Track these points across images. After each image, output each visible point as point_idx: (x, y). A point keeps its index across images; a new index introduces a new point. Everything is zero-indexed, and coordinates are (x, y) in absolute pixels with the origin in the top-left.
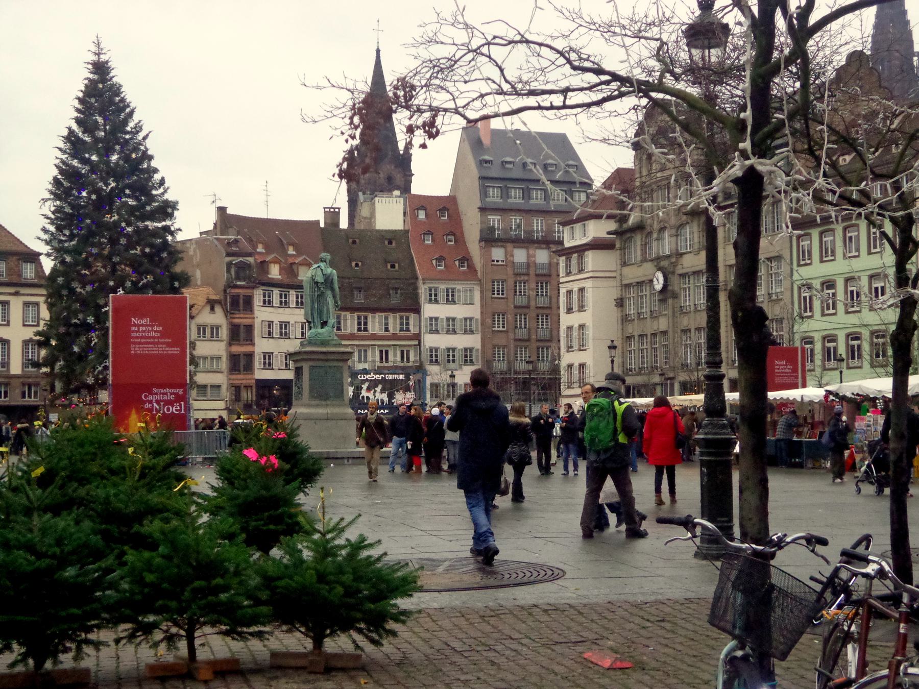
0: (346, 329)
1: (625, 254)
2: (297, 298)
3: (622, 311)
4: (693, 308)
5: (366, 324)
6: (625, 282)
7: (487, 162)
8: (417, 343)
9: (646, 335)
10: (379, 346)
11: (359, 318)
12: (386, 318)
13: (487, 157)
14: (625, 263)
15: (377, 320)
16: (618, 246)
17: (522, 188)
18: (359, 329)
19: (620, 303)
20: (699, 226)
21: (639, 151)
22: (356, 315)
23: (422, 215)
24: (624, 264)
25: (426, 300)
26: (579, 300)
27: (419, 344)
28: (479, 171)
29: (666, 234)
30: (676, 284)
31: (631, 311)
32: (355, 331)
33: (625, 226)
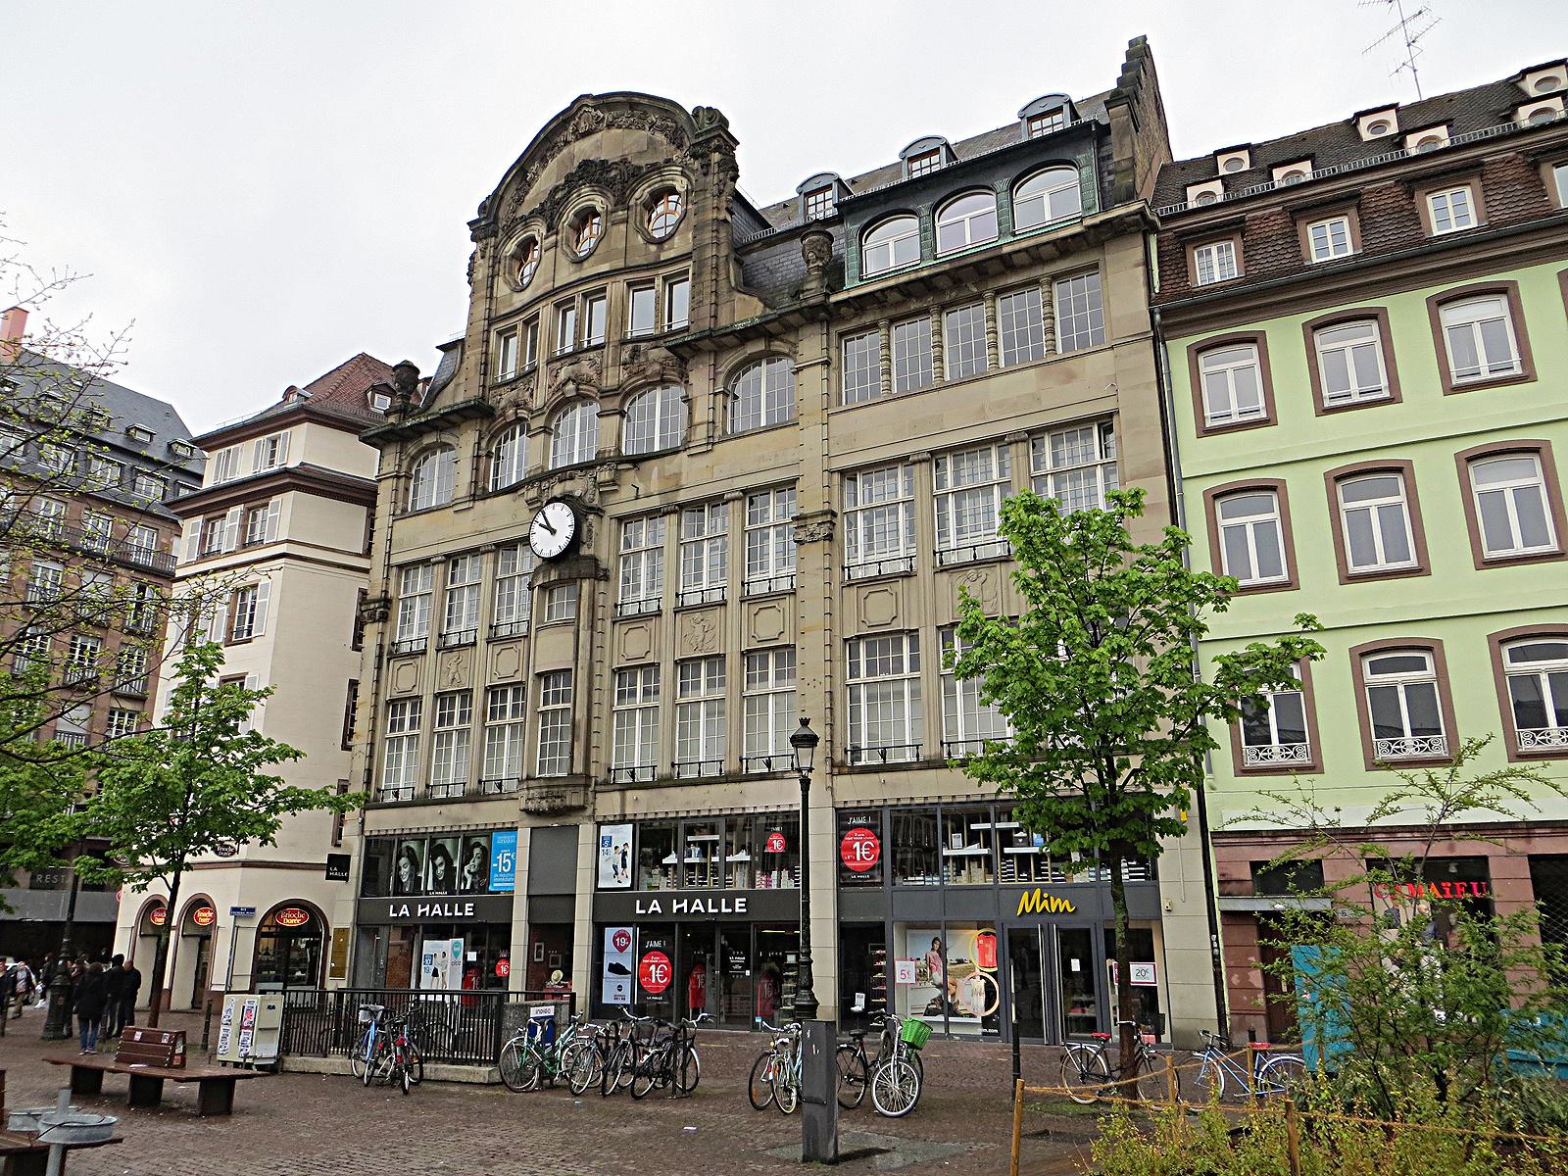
1: (407, 489)
6: (396, 560)
9: (466, 694)
19: (375, 610)
26: (231, 617)
30: (603, 545)
31: (415, 628)
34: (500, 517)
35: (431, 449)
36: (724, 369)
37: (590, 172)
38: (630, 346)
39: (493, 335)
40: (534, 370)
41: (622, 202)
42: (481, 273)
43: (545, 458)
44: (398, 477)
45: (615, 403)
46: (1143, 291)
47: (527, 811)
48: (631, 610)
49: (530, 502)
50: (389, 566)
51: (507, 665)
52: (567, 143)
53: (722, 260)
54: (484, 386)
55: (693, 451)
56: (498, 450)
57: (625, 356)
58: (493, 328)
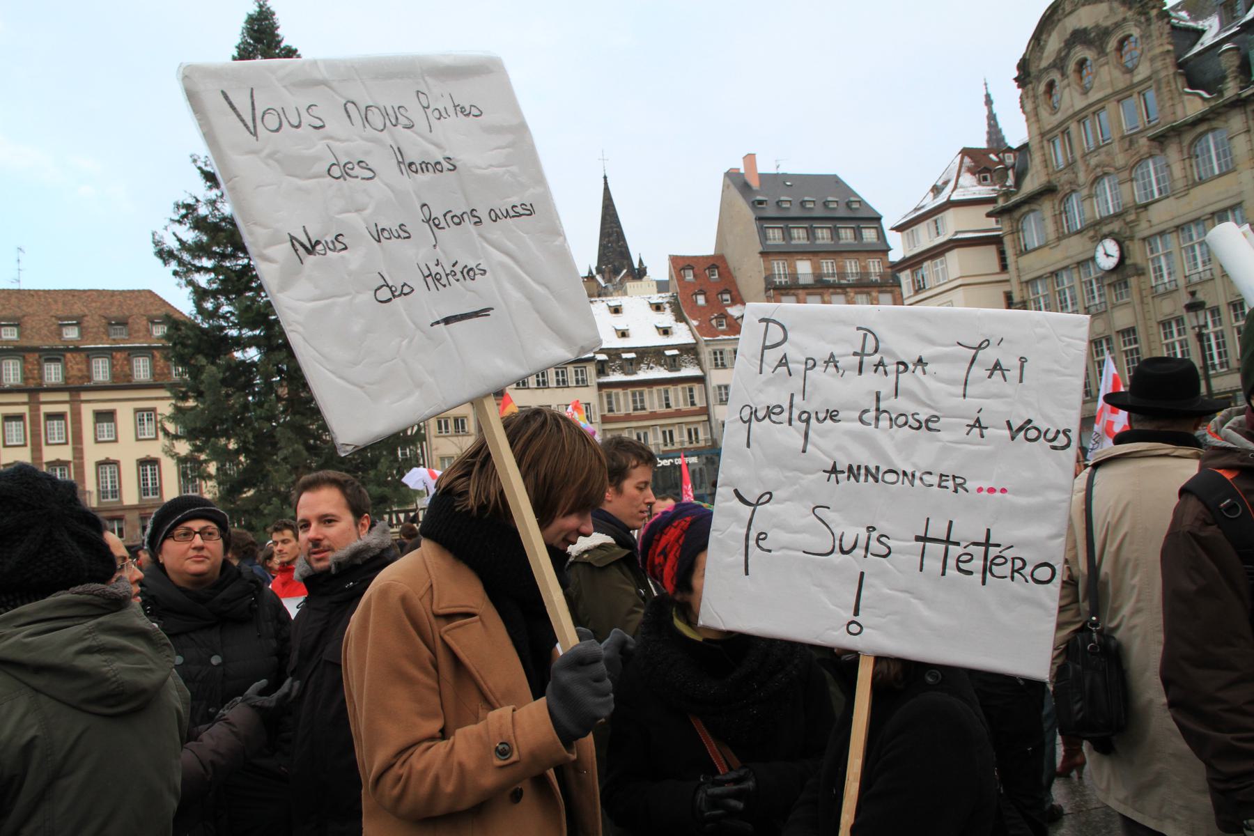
0: (619, 410)
1: (1019, 238)
2: (557, 374)
5: (642, 401)
7: (761, 202)
8: (705, 418)
10: (661, 426)
11: (634, 395)
12: (666, 392)
13: (759, 198)
14: (1021, 251)
15: (655, 396)
17: (806, 228)
18: (636, 409)
20: (1181, 151)
21: (1030, 86)
22: (629, 391)
23: (690, 276)
24: (1024, 252)
25: (711, 365)
27: (709, 420)
28: (755, 213)
29: (1106, 183)
30: (1138, 254)
32: (631, 411)
33: (1014, 199)
34: (1075, 248)
35: (1025, 215)
36: (1186, 143)
37: (1079, 37)
38: (1128, 139)
40: (1074, 161)
41: (1102, 52)
42: (1029, 107)
43: (1093, 212)
44: (1013, 233)
45: (1125, 175)
48: (1161, 289)
49: (1091, 238)
50: (1021, 283)
52: (1059, 20)
53: (1172, 76)
54: (1048, 174)
55: (1178, 195)
56: (1065, 208)
57: (1126, 145)
58: (1045, 138)
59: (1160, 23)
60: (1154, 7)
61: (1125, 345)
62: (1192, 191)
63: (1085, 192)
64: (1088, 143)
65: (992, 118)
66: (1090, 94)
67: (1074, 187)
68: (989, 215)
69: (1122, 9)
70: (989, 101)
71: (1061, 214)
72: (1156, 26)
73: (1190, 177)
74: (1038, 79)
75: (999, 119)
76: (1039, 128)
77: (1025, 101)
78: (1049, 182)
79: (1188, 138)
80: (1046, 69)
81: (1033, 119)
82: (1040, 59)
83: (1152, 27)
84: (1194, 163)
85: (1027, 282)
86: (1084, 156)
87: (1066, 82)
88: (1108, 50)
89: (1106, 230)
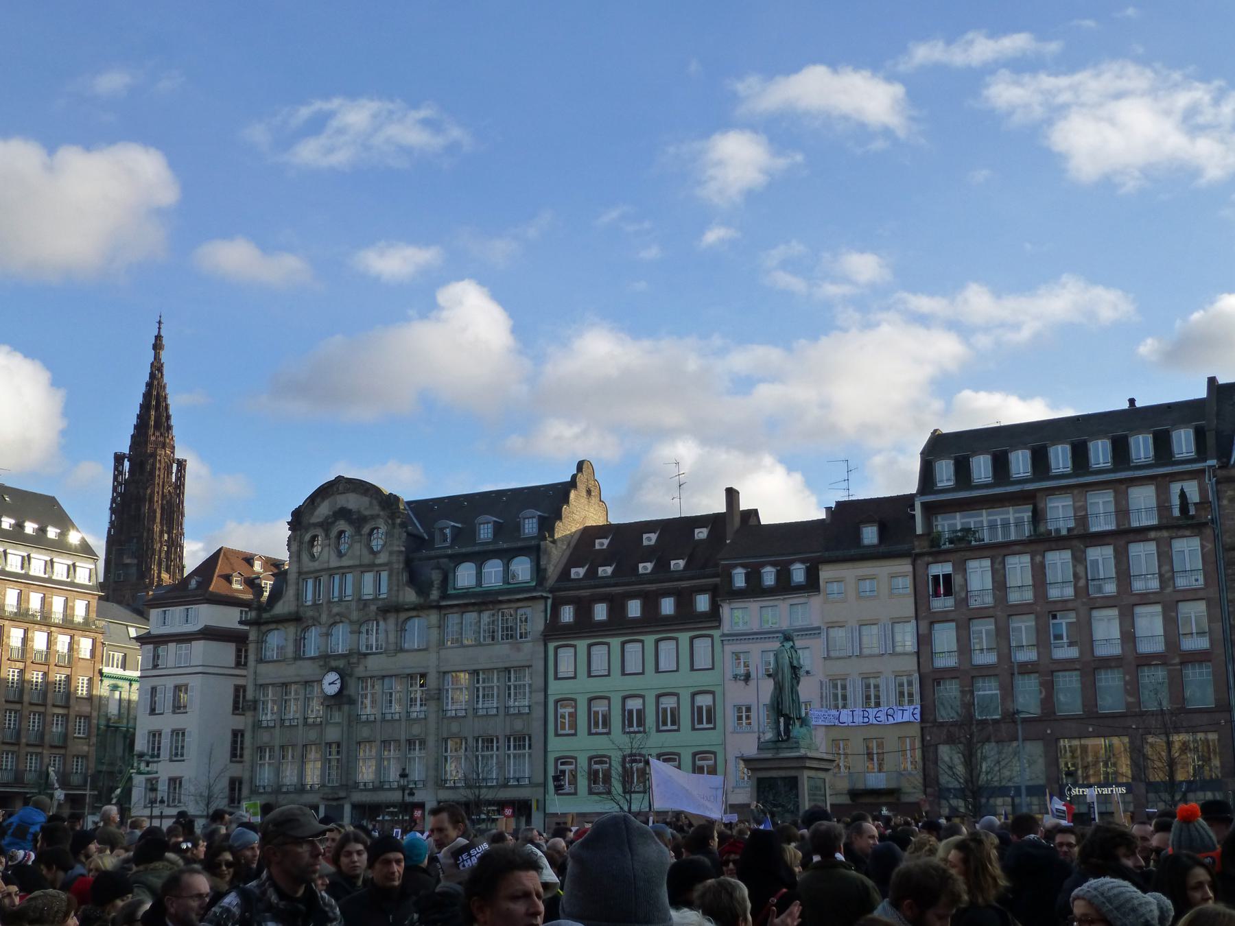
1: (262, 648)
3: (254, 716)
4: (379, 717)
6: (260, 681)
14: (261, 659)
16: (253, 636)
20: (397, 625)
21: (299, 532)
24: (260, 660)
26: (174, 700)
30: (351, 690)
33: (265, 616)
36: (400, 620)
37: (343, 513)
39: (301, 580)
41: (358, 531)
42: (294, 547)
46: (542, 622)
47: (323, 799)
49: (320, 666)
50: (256, 685)
51: (313, 735)
52: (333, 494)
56: (304, 636)
57: (361, 607)
59: (400, 530)
60: (399, 517)
61: (330, 755)
62: (399, 655)
63: (324, 630)
64: (333, 594)
65: (157, 369)
66: (343, 559)
67: (316, 623)
68: (241, 622)
69: (377, 507)
70: (158, 345)
71: (300, 639)
72: (397, 531)
73: (399, 642)
74: (307, 530)
75: (166, 370)
76: (299, 568)
77: (292, 542)
78: (297, 612)
79: (403, 616)
80: (315, 525)
81: (295, 559)
82: (312, 514)
83: (395, 531)
84: (403, 635)
85: (261, 685)
86: (329, 602)
87: (327, 542)
88: (363, 533)
89: (333, 664)
